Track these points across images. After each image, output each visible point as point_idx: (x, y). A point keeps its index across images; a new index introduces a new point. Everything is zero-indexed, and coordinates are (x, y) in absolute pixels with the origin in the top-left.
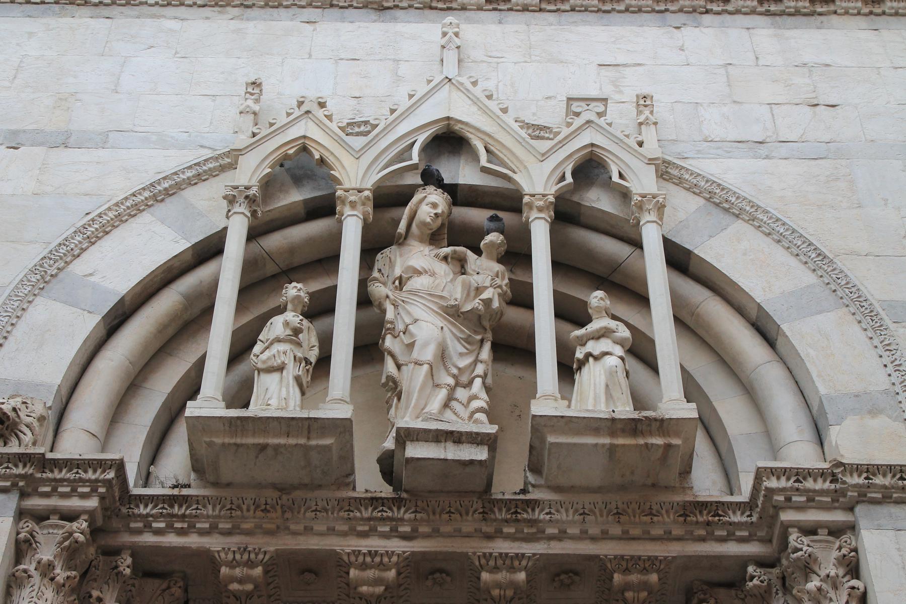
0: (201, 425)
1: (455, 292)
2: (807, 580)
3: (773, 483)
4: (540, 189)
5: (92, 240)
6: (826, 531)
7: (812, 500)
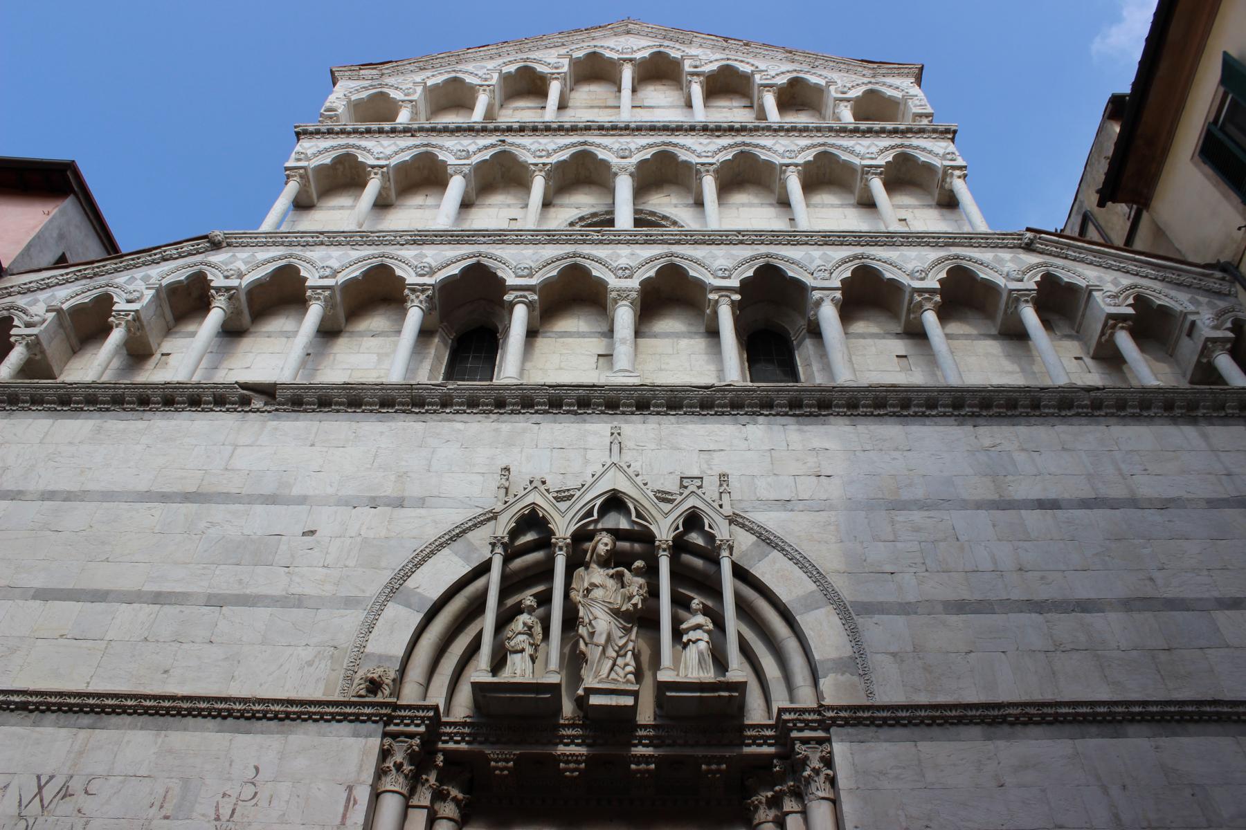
0: (478, 687)
1: (617, 601)
2: (804, 770)
3: (786, 717)
4: (664, 537)
5: (418, 565)
7: (808, 725)
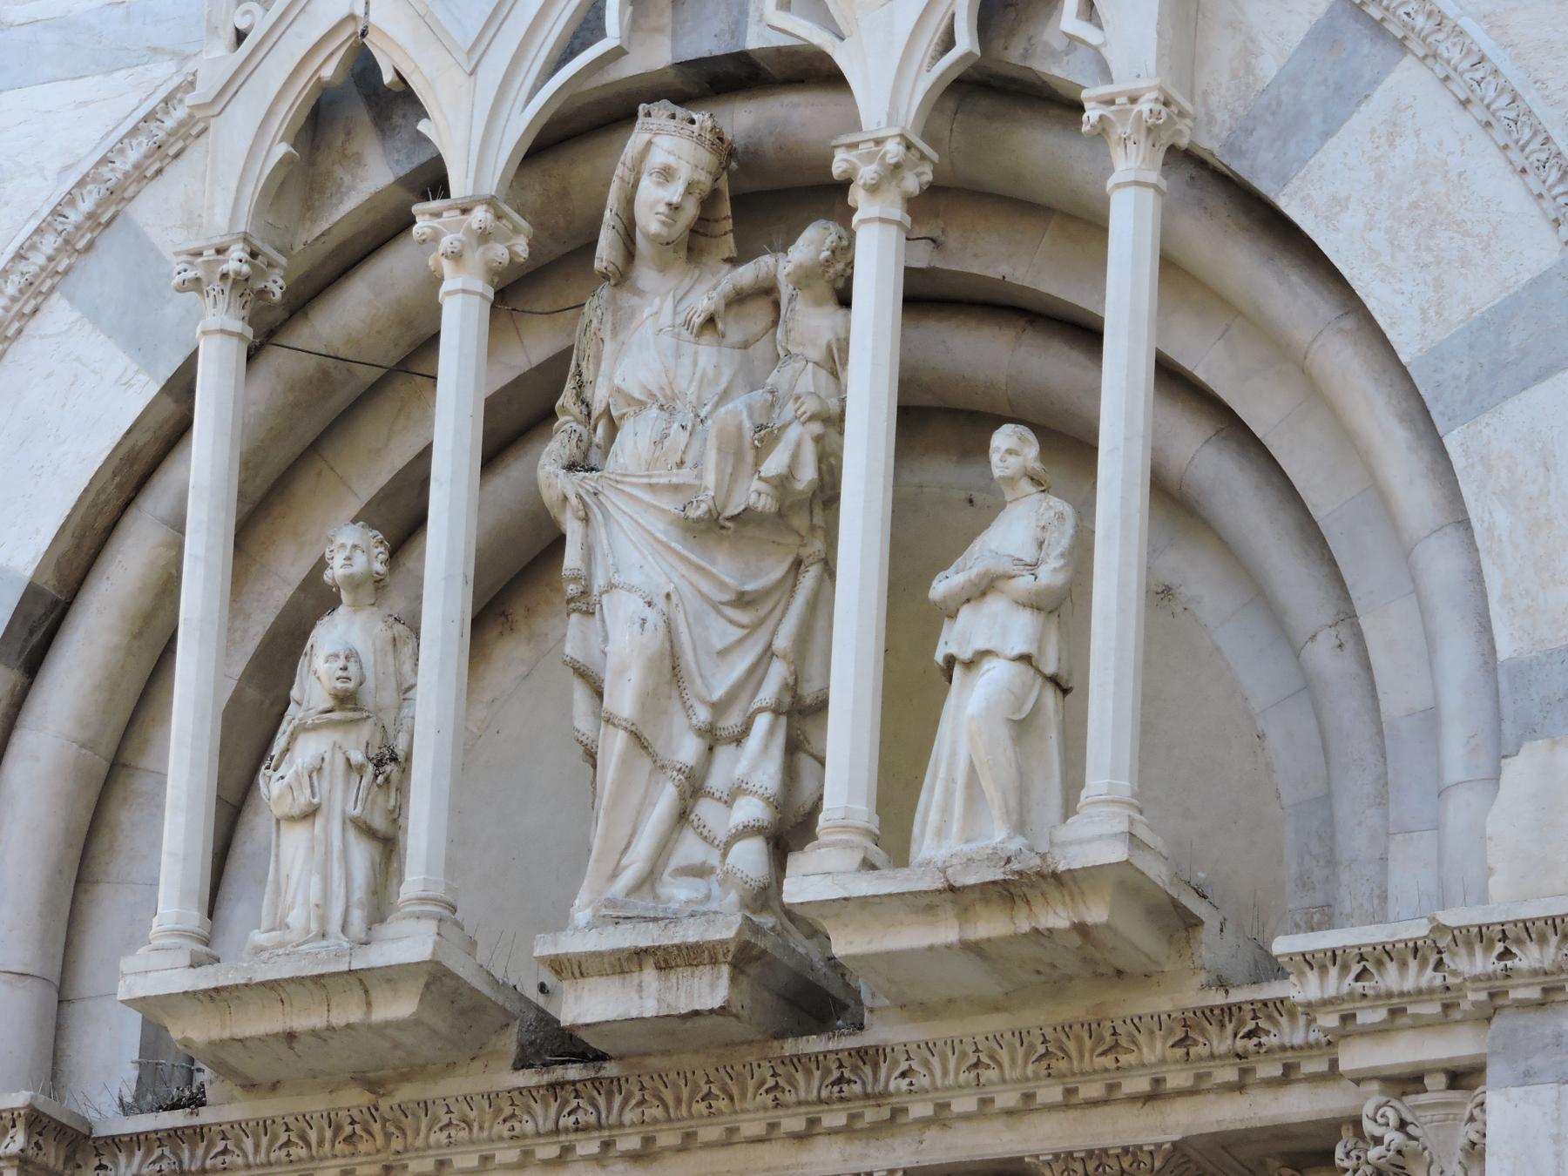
6: (1442, 1080)
